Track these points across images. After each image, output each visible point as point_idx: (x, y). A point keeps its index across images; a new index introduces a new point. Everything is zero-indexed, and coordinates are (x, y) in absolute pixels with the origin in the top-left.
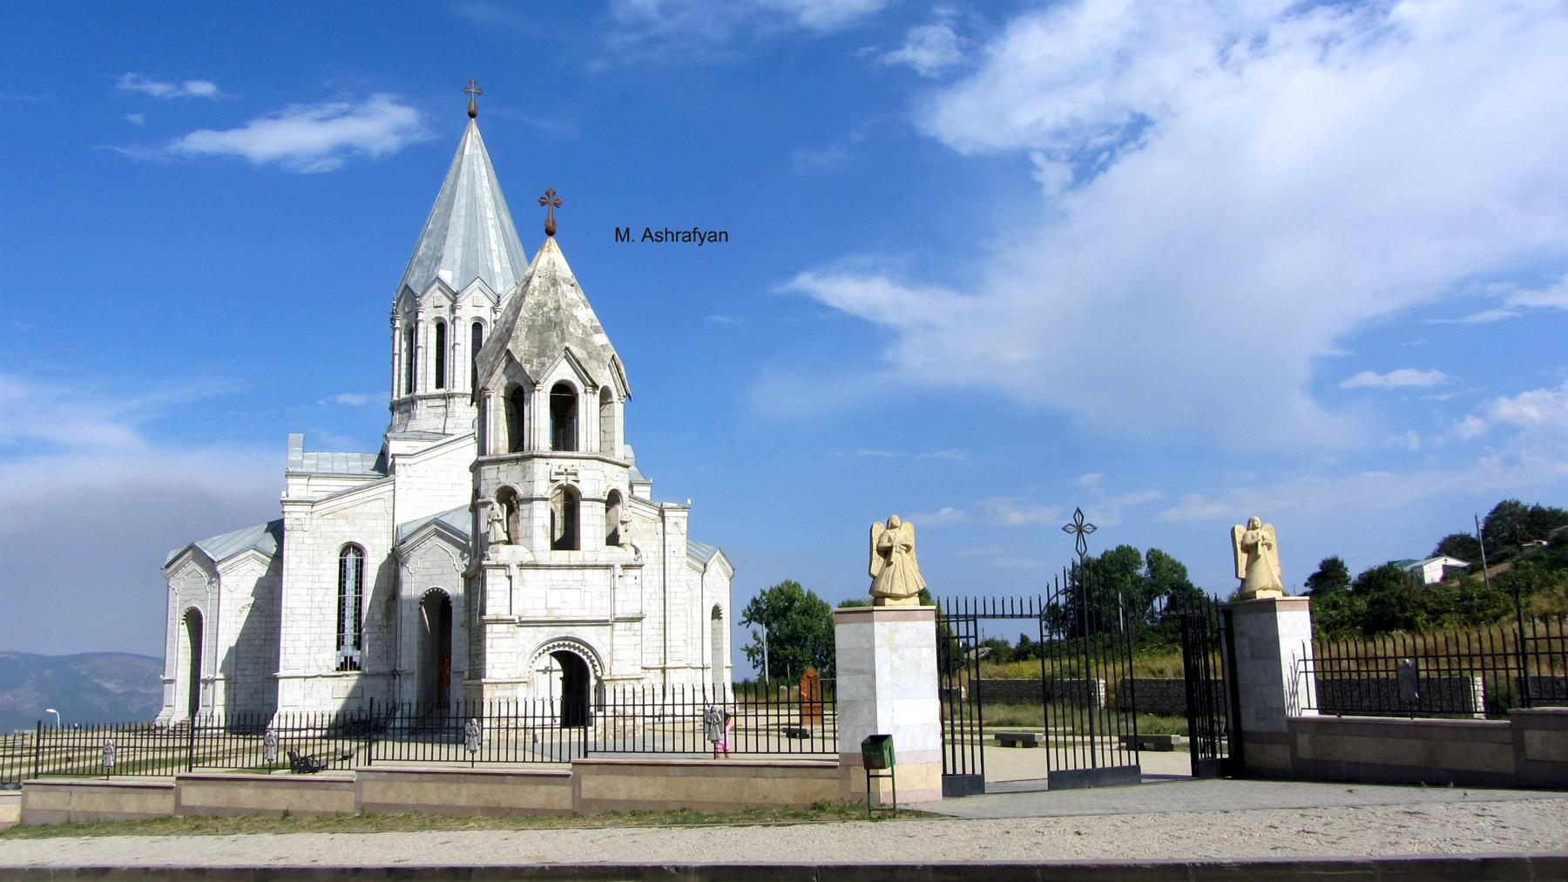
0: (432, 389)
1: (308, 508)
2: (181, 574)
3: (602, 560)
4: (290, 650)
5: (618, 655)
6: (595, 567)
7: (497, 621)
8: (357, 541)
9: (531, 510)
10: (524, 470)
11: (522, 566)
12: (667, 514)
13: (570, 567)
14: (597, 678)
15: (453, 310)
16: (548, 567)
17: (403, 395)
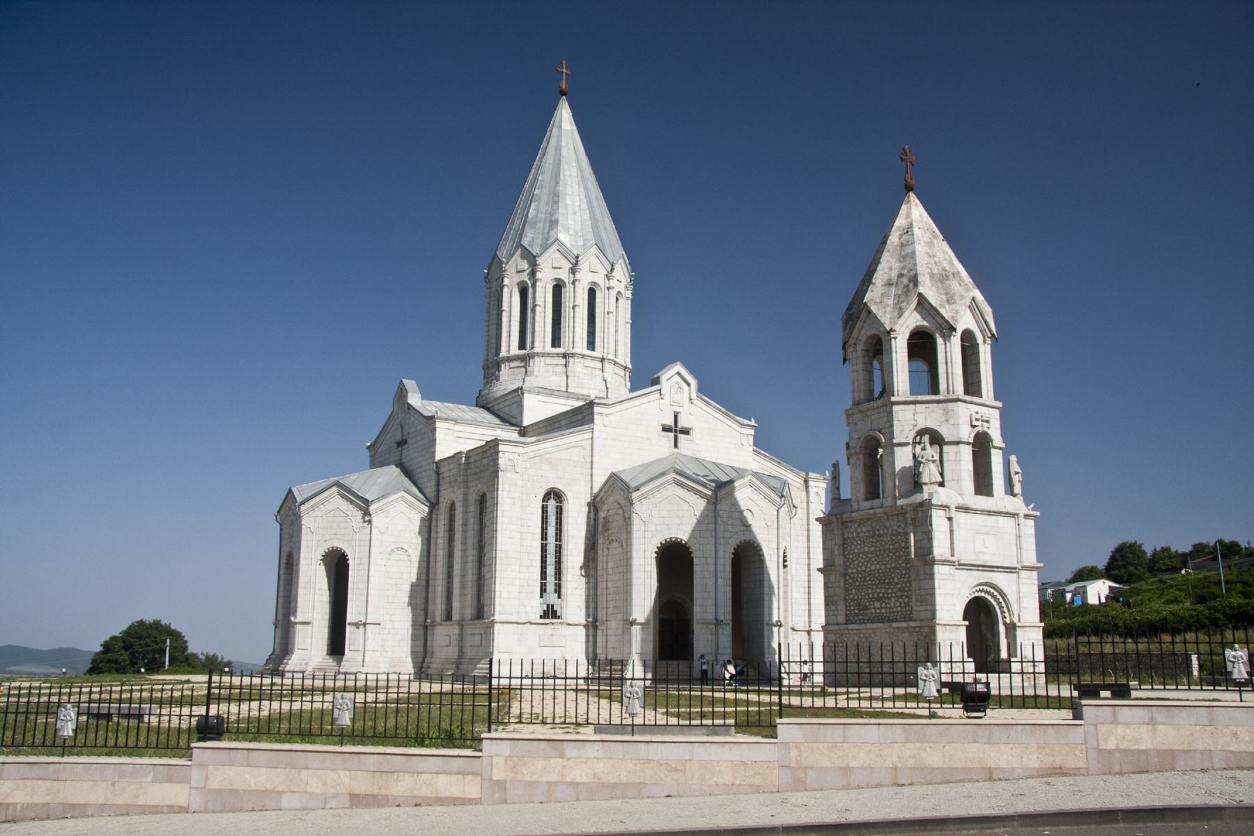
0: (549, 349)
1: (519, 450)
2: (318, 512)
3: (1010, 509)
4: (504, 595)
5: (1024, 604)
6: (1006, 514)
7: (945, 562)
8: (560, 487)
9: (957, 453)
10: (946, 412)
11: (959, 508)
12: (811, 483)
13: (990, 513)
14: (1005, 624)
15: (573, 271)
16: (975, 511)
17: (515, 351)
